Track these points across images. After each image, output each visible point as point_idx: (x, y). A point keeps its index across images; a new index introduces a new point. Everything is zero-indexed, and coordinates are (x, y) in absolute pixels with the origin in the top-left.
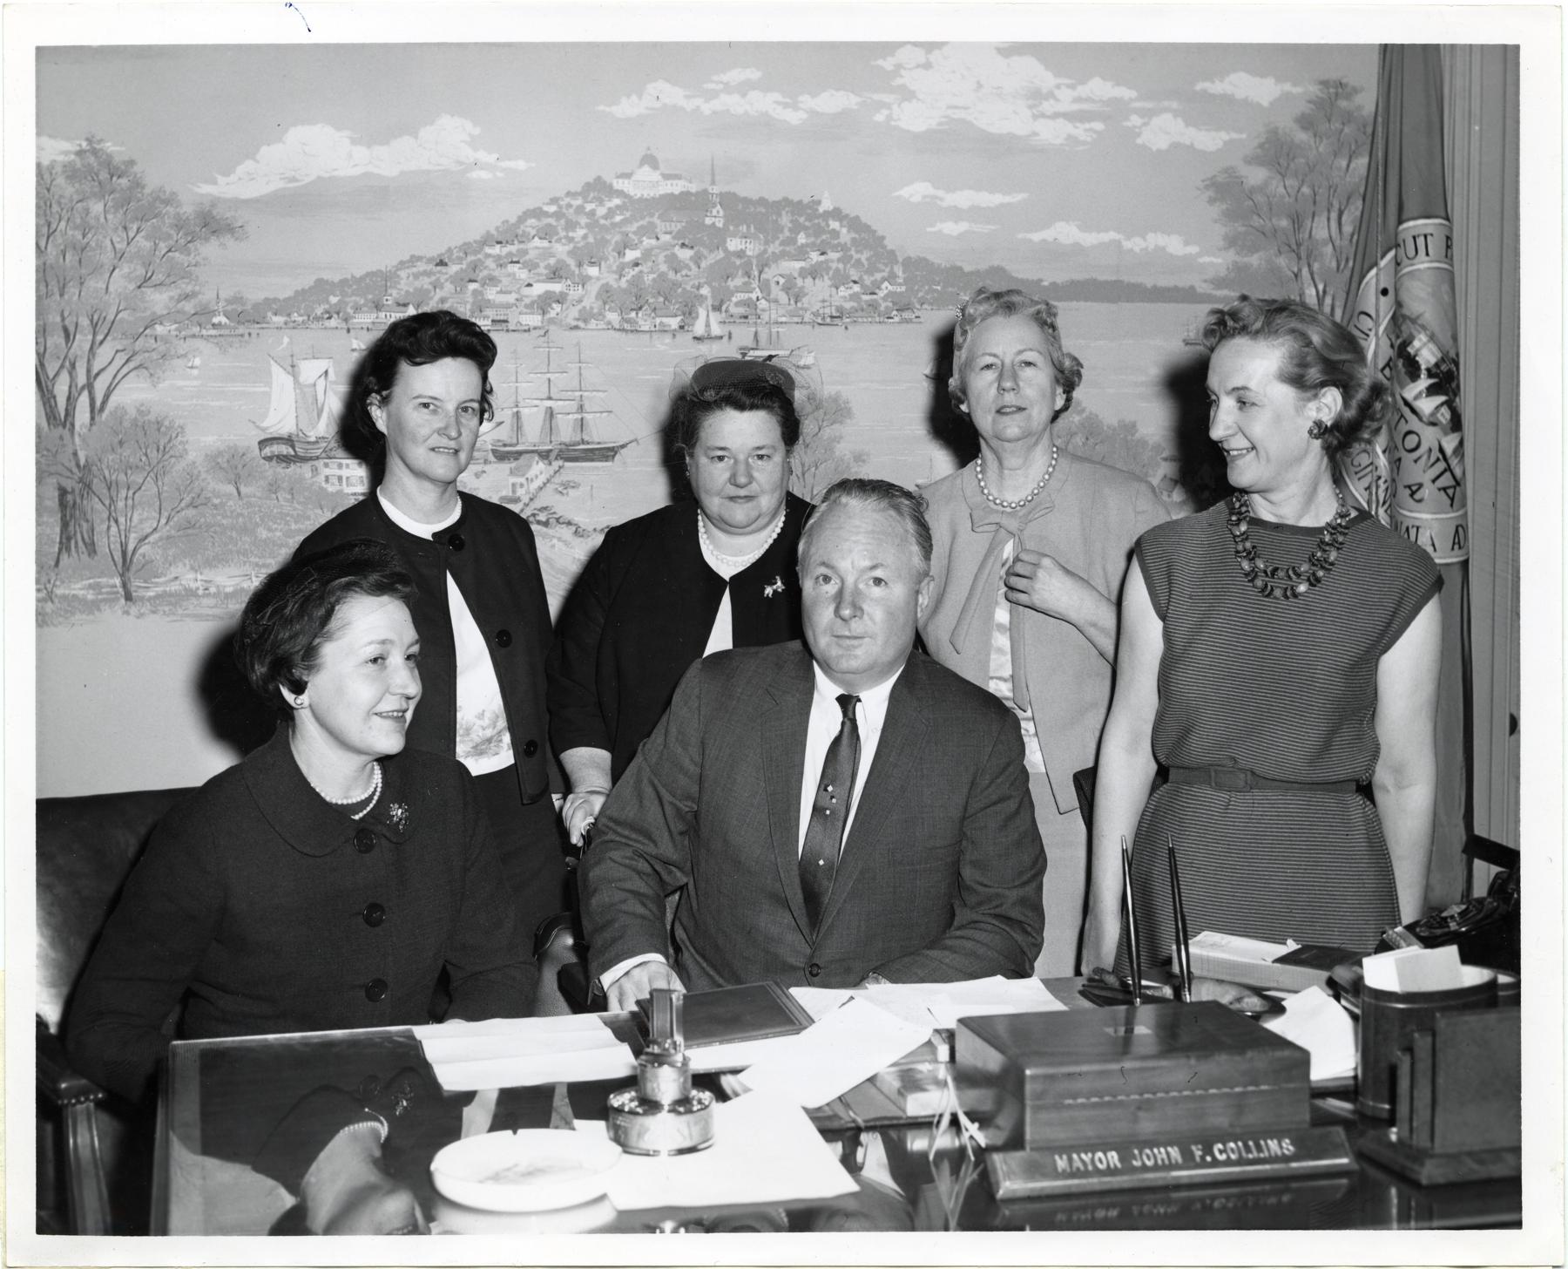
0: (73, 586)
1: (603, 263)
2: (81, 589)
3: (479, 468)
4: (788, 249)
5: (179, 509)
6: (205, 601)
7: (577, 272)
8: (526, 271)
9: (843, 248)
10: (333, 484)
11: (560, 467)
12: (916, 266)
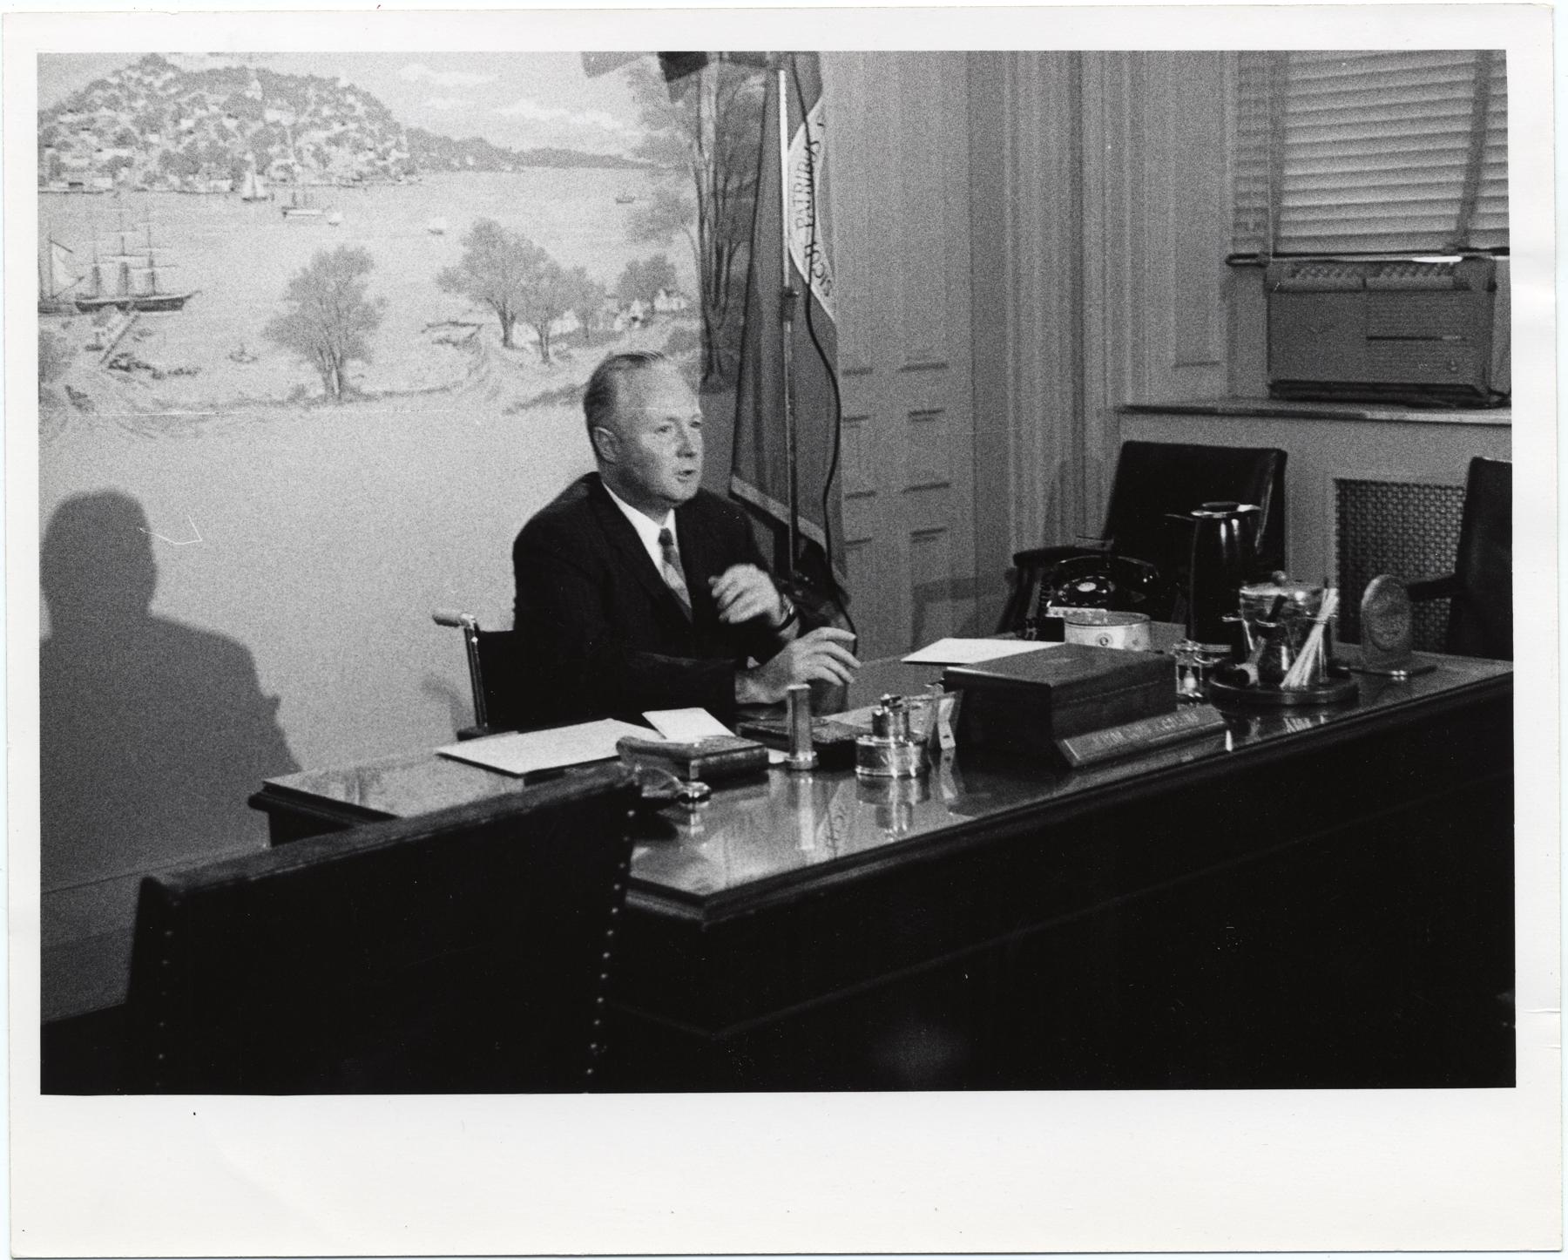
1: (162, 132)
3: (66, 319)
4: (317, 120)
7: (140, 138)
8: (95, 137)
9: (358, 119)
12: (415, 134)
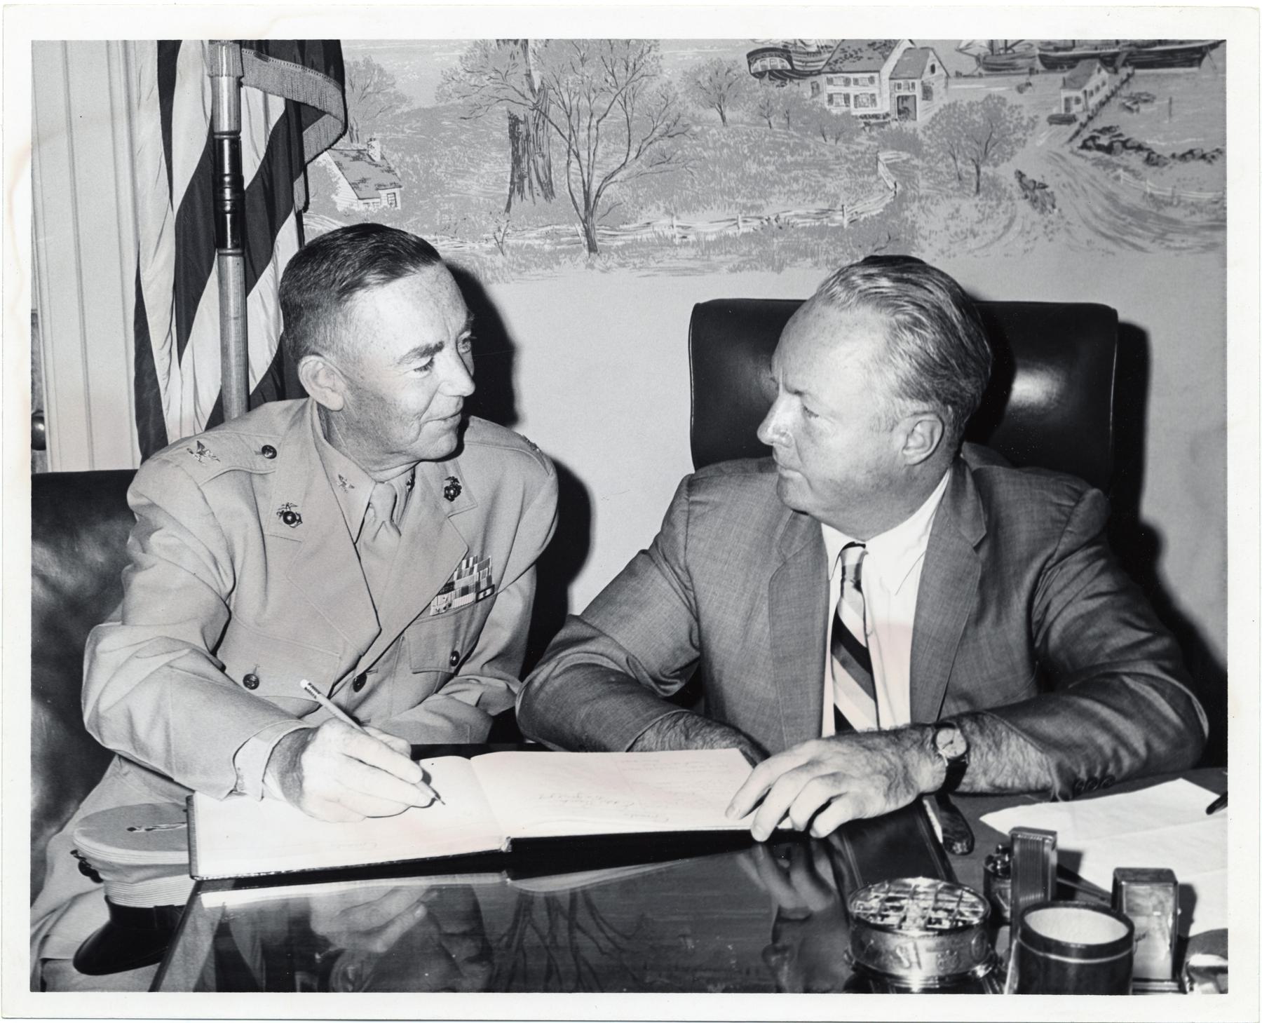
0: (530, 235)
2: (536, 238)
3: (1022, 80)
5: (650, 140)
6: (683, 252)
10: (838, 105)
11: (1129, 76)
